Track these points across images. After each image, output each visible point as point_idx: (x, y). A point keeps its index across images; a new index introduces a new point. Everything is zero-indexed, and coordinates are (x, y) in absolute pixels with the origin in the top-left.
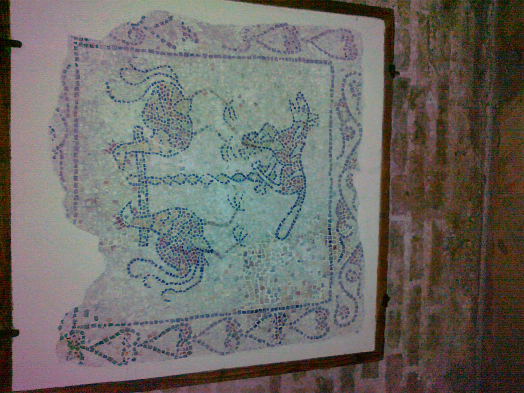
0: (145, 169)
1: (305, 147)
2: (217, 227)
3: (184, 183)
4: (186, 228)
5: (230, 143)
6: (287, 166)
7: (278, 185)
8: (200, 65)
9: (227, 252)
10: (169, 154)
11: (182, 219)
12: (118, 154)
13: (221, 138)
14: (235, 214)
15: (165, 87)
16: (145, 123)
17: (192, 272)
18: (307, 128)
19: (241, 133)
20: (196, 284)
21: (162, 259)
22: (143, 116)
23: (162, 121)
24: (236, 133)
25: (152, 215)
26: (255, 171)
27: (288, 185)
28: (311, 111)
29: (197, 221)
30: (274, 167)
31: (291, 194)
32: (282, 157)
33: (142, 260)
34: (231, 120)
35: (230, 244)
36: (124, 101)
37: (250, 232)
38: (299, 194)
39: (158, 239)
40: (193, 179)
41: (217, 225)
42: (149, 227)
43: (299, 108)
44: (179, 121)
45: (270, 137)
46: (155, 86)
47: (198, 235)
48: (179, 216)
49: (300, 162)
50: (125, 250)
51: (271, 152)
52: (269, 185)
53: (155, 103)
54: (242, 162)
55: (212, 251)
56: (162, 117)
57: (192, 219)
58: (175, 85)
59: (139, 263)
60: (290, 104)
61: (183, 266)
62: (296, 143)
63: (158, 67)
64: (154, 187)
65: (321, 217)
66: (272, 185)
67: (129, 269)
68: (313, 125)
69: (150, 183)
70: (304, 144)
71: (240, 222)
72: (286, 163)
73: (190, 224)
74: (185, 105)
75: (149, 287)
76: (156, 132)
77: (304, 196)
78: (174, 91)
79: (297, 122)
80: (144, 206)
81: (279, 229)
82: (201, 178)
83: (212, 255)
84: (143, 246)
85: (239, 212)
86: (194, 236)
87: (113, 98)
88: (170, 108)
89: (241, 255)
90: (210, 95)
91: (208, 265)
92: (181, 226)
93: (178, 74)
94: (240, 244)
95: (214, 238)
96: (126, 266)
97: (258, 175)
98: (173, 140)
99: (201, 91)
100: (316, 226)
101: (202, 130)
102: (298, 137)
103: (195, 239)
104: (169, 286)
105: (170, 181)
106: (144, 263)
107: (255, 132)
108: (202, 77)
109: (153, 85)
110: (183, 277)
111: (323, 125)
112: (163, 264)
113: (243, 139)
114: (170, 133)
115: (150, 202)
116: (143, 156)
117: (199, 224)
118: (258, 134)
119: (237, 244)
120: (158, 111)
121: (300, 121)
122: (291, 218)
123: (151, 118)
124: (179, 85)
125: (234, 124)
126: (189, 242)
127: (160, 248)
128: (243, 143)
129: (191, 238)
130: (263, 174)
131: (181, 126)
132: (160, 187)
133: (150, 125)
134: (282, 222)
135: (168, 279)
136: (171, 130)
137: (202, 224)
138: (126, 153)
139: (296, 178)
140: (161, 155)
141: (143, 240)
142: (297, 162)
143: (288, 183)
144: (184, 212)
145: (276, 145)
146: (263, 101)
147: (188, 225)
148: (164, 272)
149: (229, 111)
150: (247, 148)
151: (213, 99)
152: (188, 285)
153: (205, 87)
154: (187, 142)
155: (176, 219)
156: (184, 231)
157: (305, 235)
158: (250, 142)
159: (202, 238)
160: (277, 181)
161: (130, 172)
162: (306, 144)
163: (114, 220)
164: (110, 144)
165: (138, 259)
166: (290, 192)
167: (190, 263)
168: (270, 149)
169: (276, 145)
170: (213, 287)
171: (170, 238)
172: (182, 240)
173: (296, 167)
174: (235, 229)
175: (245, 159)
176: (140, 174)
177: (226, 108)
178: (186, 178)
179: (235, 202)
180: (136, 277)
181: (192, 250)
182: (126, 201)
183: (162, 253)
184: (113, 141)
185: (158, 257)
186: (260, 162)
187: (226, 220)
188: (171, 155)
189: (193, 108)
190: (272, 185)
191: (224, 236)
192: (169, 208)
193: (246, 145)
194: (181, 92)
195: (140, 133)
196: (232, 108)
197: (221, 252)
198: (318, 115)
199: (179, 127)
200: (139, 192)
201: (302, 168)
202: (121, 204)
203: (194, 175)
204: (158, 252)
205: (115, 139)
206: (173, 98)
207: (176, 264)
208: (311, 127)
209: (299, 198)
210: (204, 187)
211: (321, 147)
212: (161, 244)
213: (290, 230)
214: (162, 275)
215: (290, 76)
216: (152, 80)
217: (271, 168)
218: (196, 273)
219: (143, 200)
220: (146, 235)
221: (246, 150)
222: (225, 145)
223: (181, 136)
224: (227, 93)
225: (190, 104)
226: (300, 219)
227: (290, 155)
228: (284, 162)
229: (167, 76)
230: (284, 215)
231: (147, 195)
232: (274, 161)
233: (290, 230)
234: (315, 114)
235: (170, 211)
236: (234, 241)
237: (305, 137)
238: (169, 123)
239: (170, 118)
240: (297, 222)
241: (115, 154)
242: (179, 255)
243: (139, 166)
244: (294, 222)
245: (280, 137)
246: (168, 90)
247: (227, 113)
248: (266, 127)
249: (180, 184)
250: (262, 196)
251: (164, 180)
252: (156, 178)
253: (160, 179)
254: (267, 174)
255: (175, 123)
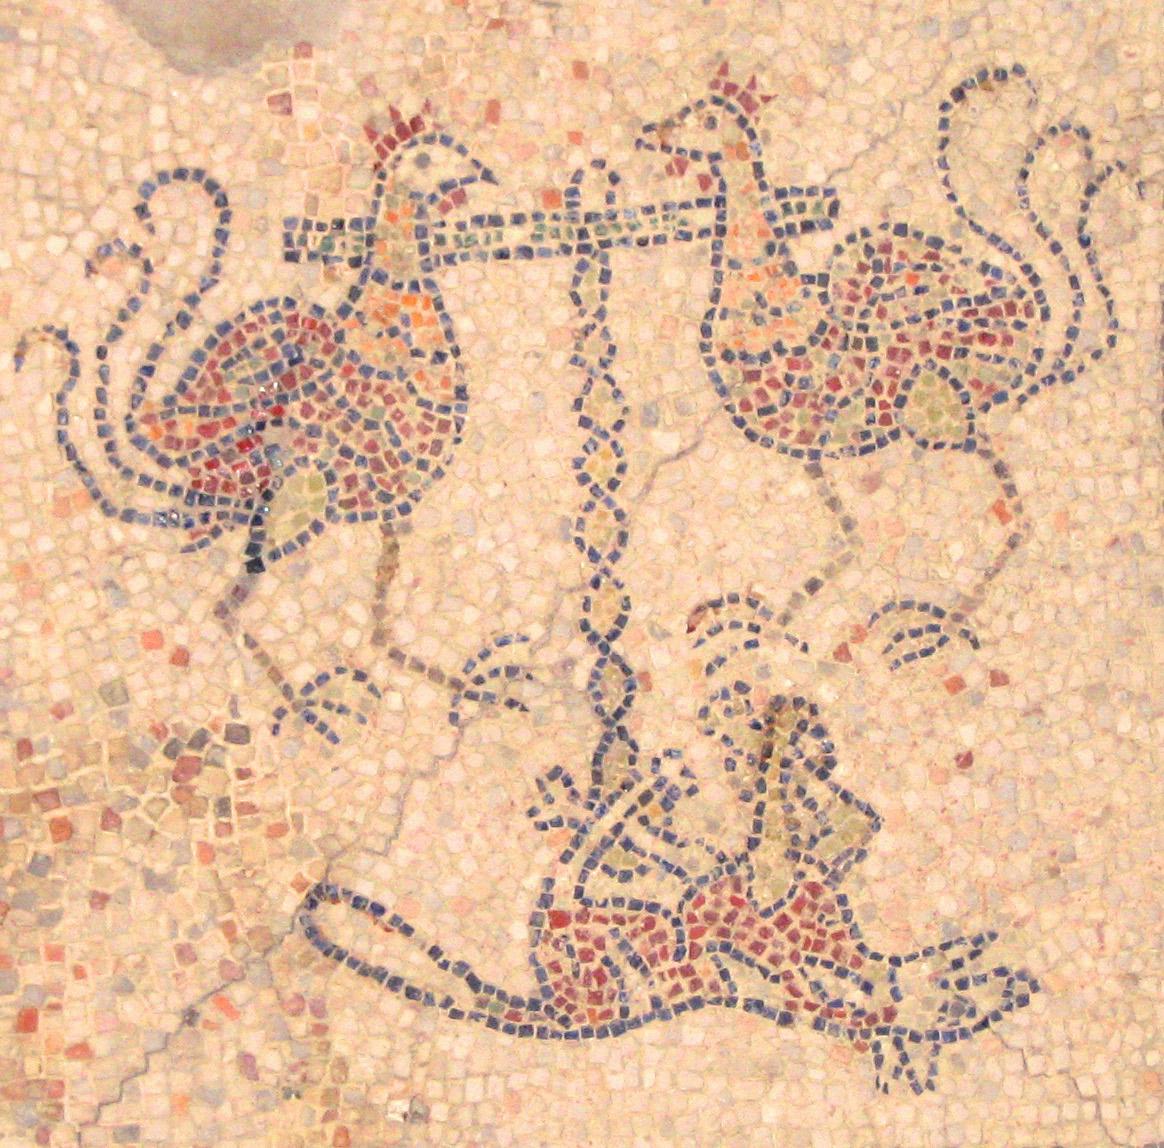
0: (642, 243)
1: (771, 1025)
2: (368, 590)
3: (585, 422)
4: (368, 435)
5: (773, 637)
6: (672, 937)
7: (579, 893)
8: (1129, 485)
9: (251, 643)
10: (715, 352)
11: (414, 415)
12: (711, 123)
13: (797, 596)
14: (436, 675)
15: (1019, 325)
16: (851, 239)
17: (153, 470)
18: (866, 1034)
19: (824, 693)
20: (96, 495)
21: (224, 328)
22: (884, 226)
23: (864, 314)
24: (826, 669)
25: (435, 276)
26: (643, 766)
27: (578, 945)
28: (948, 1049)
29: (401, 489)
30: (668, 867)
31: (533, 960)
32: (718, 904)
33: (221, 235)
34: (878, 642)
35: (286, 655)
36: (944, 143)
37: (344, 753)
38: (534, 1005)
39: (318, 310)
40: (601, 467)
41: (381, 592)
42: (377, 262)
43: (962, 984)
44: (868, 392)
45: (814, 840)
46: (1023, 279)
47: (333, 494)
48: (427, 404)
49: (697, 1003)
50: (272, 159)
51: (740, 847)
52: (576, 843)
53: (943, 280)
54: (689, 705)
55: (255, 566)
56: (882, 313)
57: (411, 468)
58: (1031, 370)
59: (208, 223)
60: (978, 940)
61: (187, 426)
62: (788, 976)
63: (1105, 292)
64: (560, 286)
65: (417, 1130)
66: (580, 856)
67: (181, 174)
68: (879, 1061)
69: (582, 266)
70: (786, 1020)
71: (394, 700)
72: (686, 928)
73: (388, 454)
74: (945, 418)
75: (90, 269)
76: (816, 289)
77: (526, 1031)
78: (1005, 365)
79: (892, 978)
80: (471, 241)
81: (358, 903)
82: (609, 502)
83: (235, 569)
84: (288, 241)
85: (444, 696)
86: (330, 478)
87: (959, 94)
88: (925, 347)
89: (234, 713)
90: (994, 536)
91: (189, 549)
92: (380, 412)
93: (1080, 385)
94: (287, 705)
95: (316, 576)
96: (191, 162)
97: (626, 786)
98: (780, 365)
99: (1011, 490)
100: (370, 1106)
101: (834, 503)
102: (816, 985)
103: (314, 486)
104: (88, 362)
105: (593, 360)
106: (205, 245)
107: (831, 763)
108: (1078, 496)
109: (1027, 269)
110: (130, 427)
111: (881, 1120)
112: (197, 335)
113: (798, 702)
114: (811, 350)
115: (492, 266)
116: (704, 233)
117: (386, 498)
118: (823, 775)
119: (287, 691)
120: (911, 297)
121: (896, 995)
122: (414, 965)
123: (878, 266)
124: (1034, 390)
125: (867, 653)
126: (299, 453)
127: (276, 317)
128: (778, 703)
129: (320, 466)
130: (632, 810)
131: (845, 402)
132: (562, 314)
133: (844, 259)
134: (396, 920)
135: (125, 360)
136: (827, 354)
137: (387, 515)
138: (715, 157)
139: (612, 984)
140: (710, 314)
141: (315, 240)
142: (696, 984)
143: (590, 945)
144: (444, 426)
145: (772, 876)
146: (982, 799)
147: (386, 445)
148: (158, 338)
149: (932, 628)
150: (756, 726)
151: (979, 548)
152: (91, 451)
153: (1032, 508)
154: (774, 434)
155: (412, 390)
156: (357, 427)
157: (326, 1047)
158: (782, 739)
159: (321, 516)
160: (600, 886)
161: (629, 178)
162: (786, 1033)
163: (409, 109)
164: (753, 84)
165: (225, 217)
166: (546, 953)
167: (200, 463)
168: (753, 844)
169: (772, 876)
170: (77, 574)
171: (321, 365)
172: (313, 419)
173: (670, 983)
174: (360, 676)
175: (704, 712)
176: (621, 219)
177: (939, 613)
178: (605, 435)
179: (495, 673)
180: (142, 211)
181: (264, 472)
182: (493, 159)
183: (251, 327)
184: (766, 99)
185: (229, 311)
186: (692, 791)
187: (403, 633)
188: (710, 362)
189: (931, 458)
190: (580, 856)
191: (328, 626)
192: (464, 358)
193: (770, 721)
194: (1001, 397)
195: (808, 216)
196: (942, 642)
197: (248, 614)
198: (931, 1086)
199: (839, 396)
200: (537, 216)
201: (665, 1016)
202: (483, 136)
203: (621, 469)
204: (257, 308)
205: (772, 108)
206: (972, 360)
207: (199, 392)
208: (870, 1054)
209: (517, 1002)
210: (566, 520)
211: (770, 1114)
212: (293, 320)
213: (353, 963)
214: (147, 327)
215: (1111, 935)
216: (1044, 264)
217: (661, 848)
218: (150, 491)
219: (500, 237)
220: (337, 251)
221: (744, 720)
222: (766, 614)
223: (799, 402)
224: (1010, 617)
225: (950, 440)
226: (408, 1017)
227: (726, 948)
228: (692, 919)
229: (1072, 333)
230: (431, 932)
231: (526, 252)
232: (693, 864)
233: (353, 963)
234: (933, 1070)
235: (450, 360)
236: (301, 675)
237: (818, 1025)
238: (857, 344)
239: (882, 351)
240: (393, 1002)
241: (711, 108)
242: (239, 408)
243: (659, 214)
244: (395, 983)
245: (814, 889)
246: (1008, 340)
247: (916, 619)
248: (863, 818)
249: (578, 404)
250: (523, 807)
251: (596, 332)
252: (604, 296)
253: (601, 314)
254: (632, 829)
255: (858, 374)
